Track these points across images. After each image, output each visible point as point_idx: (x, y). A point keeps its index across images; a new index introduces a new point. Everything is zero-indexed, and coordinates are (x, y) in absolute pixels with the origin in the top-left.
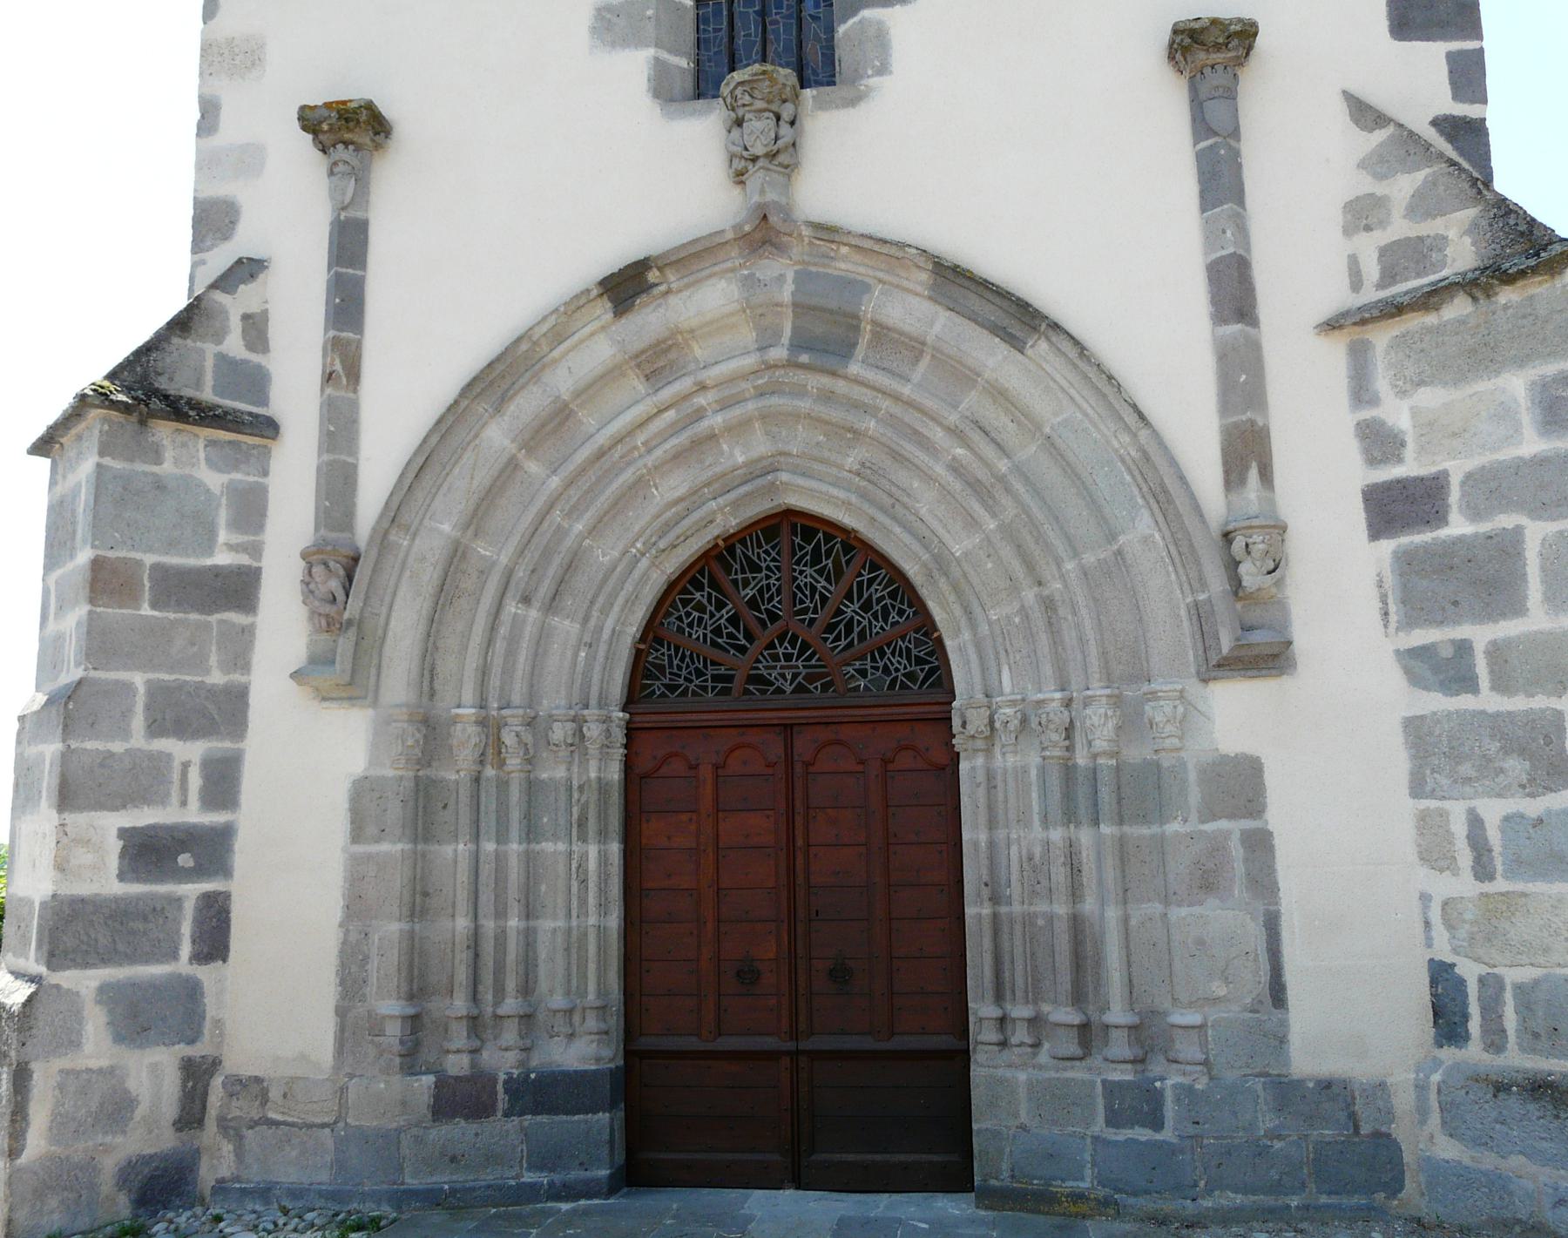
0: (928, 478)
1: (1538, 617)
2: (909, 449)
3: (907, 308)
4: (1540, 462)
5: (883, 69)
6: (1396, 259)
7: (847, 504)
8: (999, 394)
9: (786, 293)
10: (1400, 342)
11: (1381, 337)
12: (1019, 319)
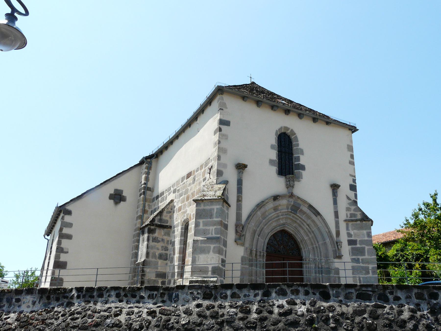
0: (303, 229)
1: (366, 256)
2: (302, 225)
3: (305, 209)
4: (367, 240)
5: (302, 178)
6: (352, 215)
7: (293, 231)
8: (313, 221)
9: (292, 204)
10: (352, 224)
11: (350, 224)
12: (317, 213)
